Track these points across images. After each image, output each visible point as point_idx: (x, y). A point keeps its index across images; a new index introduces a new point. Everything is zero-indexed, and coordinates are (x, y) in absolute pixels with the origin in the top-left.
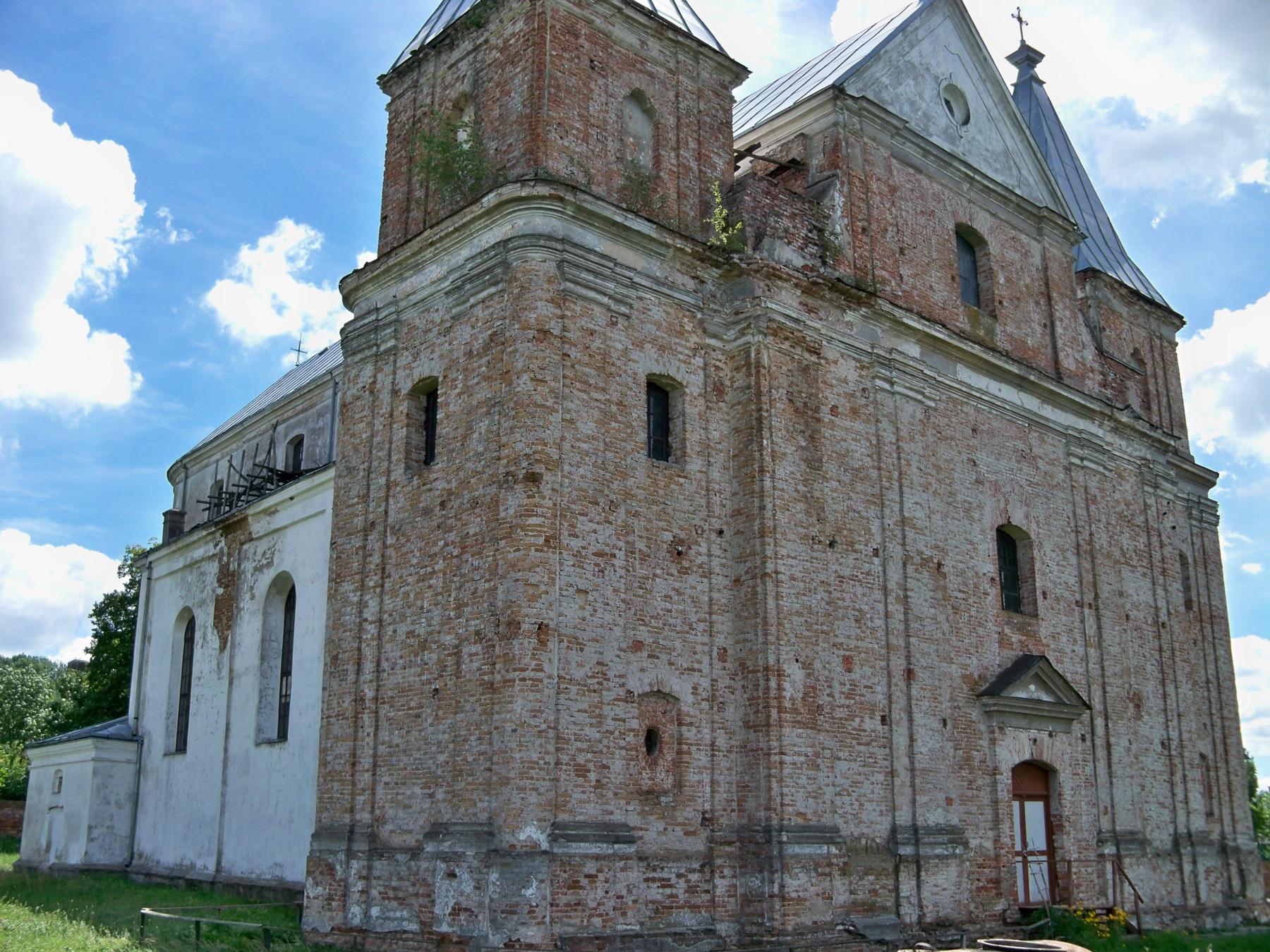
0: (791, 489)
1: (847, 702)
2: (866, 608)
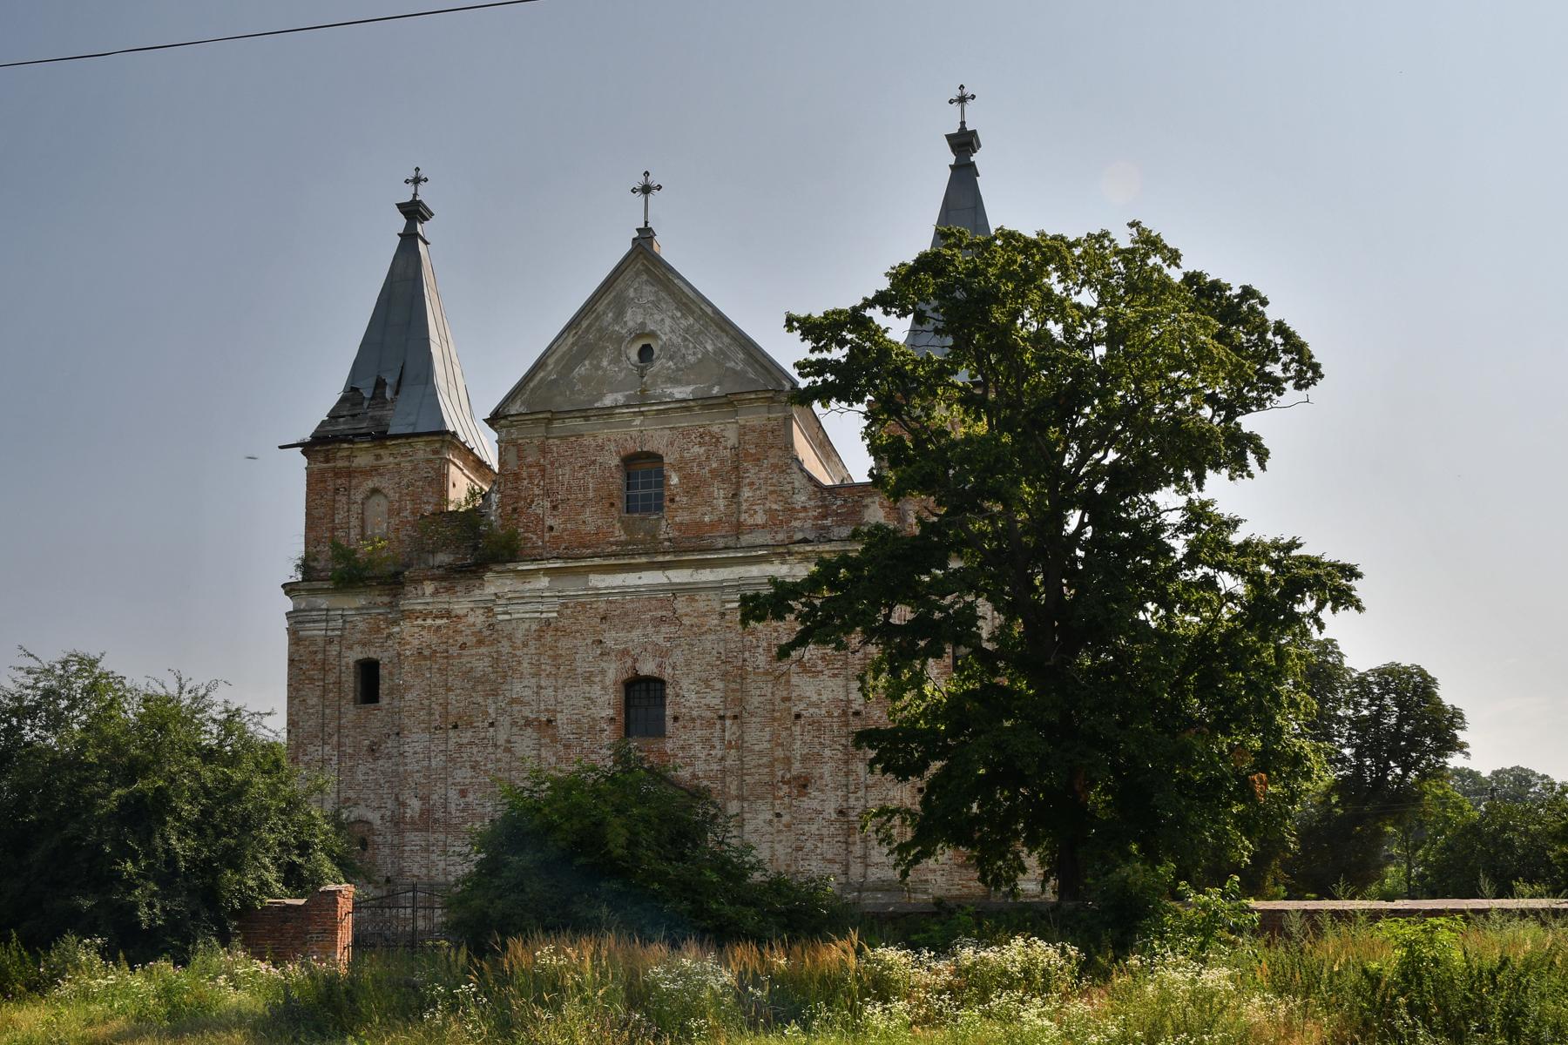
0: (417, 705)
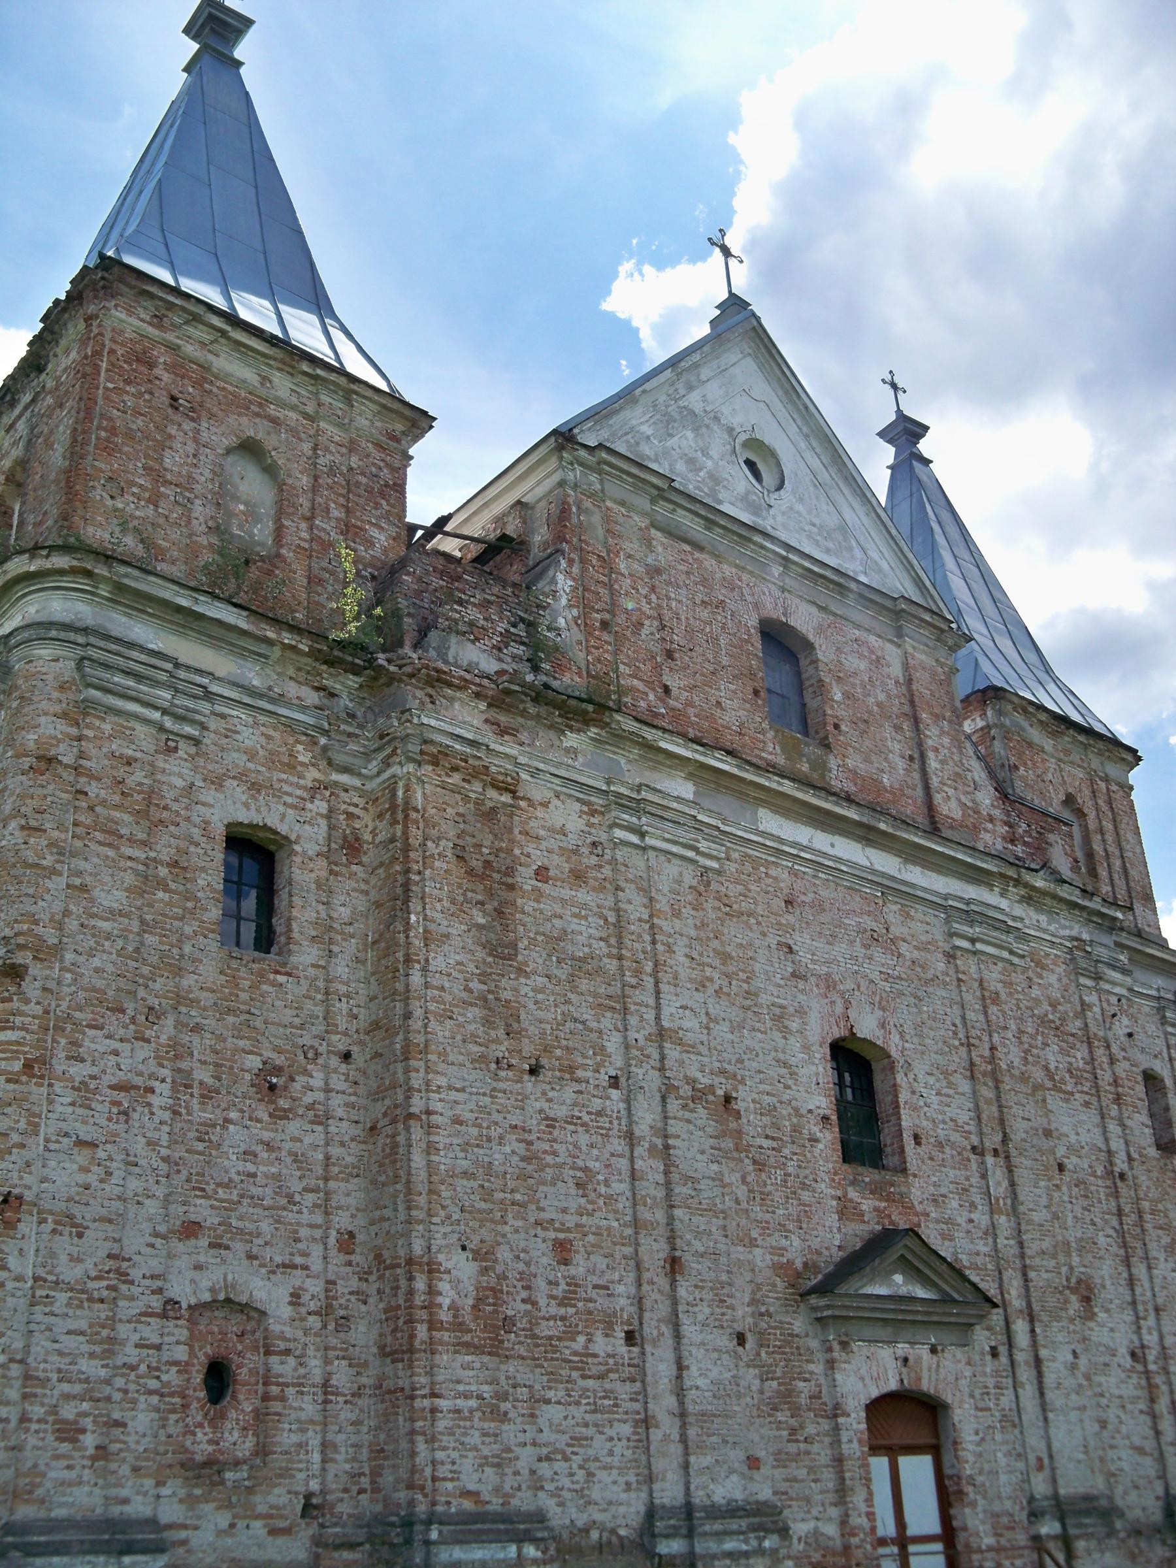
0: (457, 989)
1: (562, 1311)
2: (595, 1165)
